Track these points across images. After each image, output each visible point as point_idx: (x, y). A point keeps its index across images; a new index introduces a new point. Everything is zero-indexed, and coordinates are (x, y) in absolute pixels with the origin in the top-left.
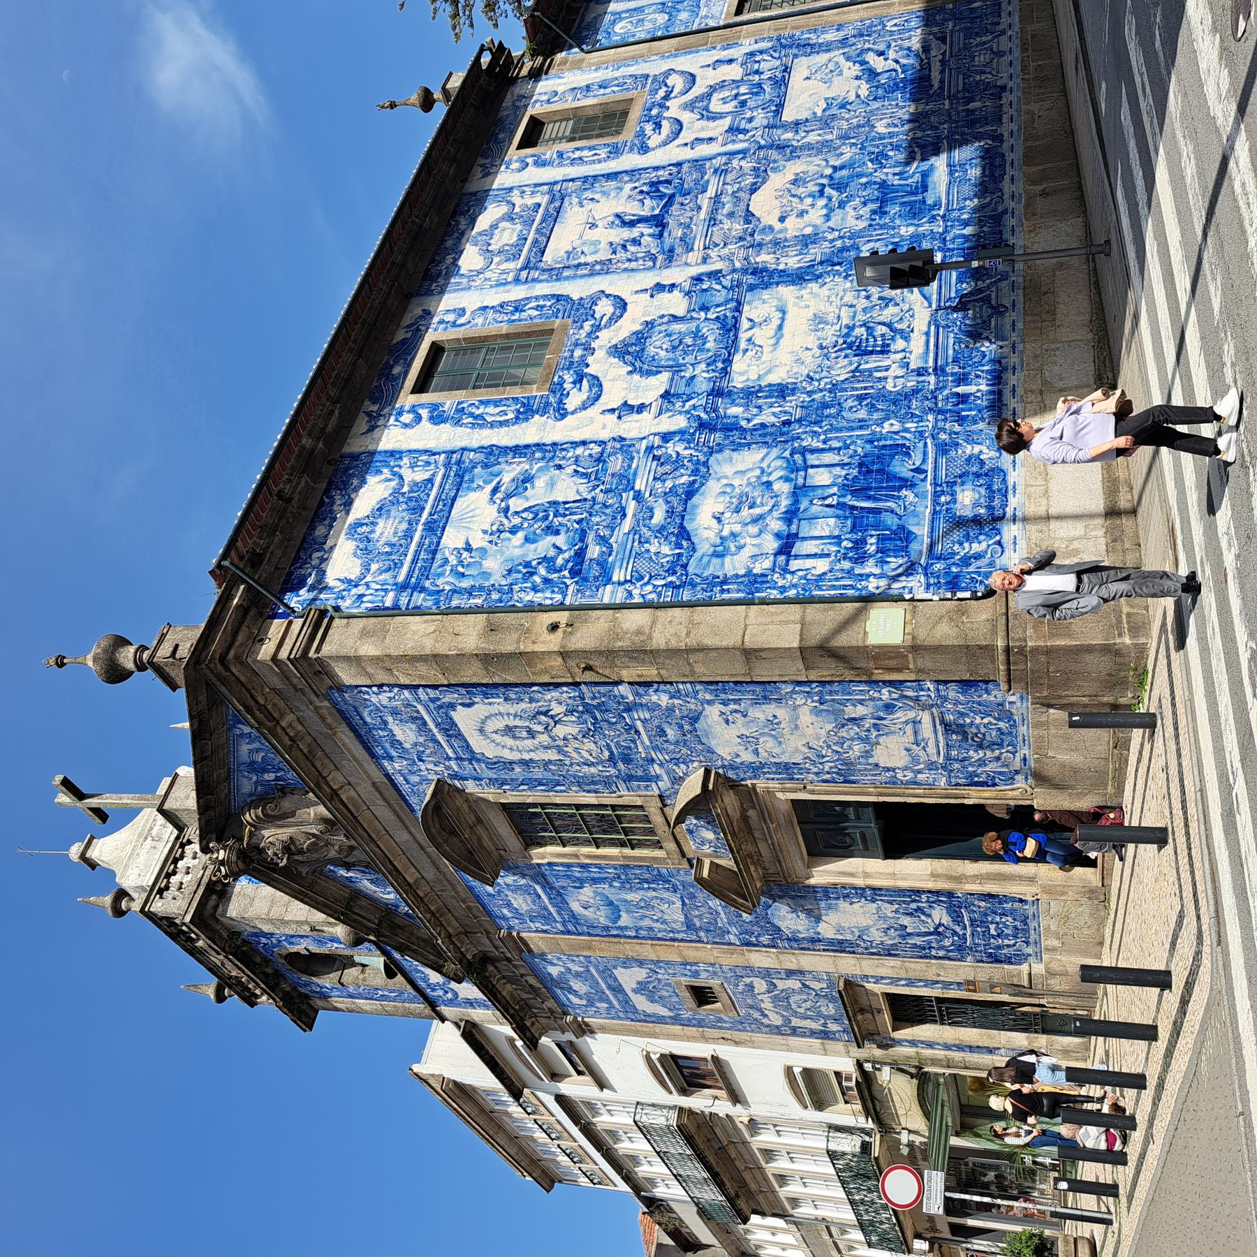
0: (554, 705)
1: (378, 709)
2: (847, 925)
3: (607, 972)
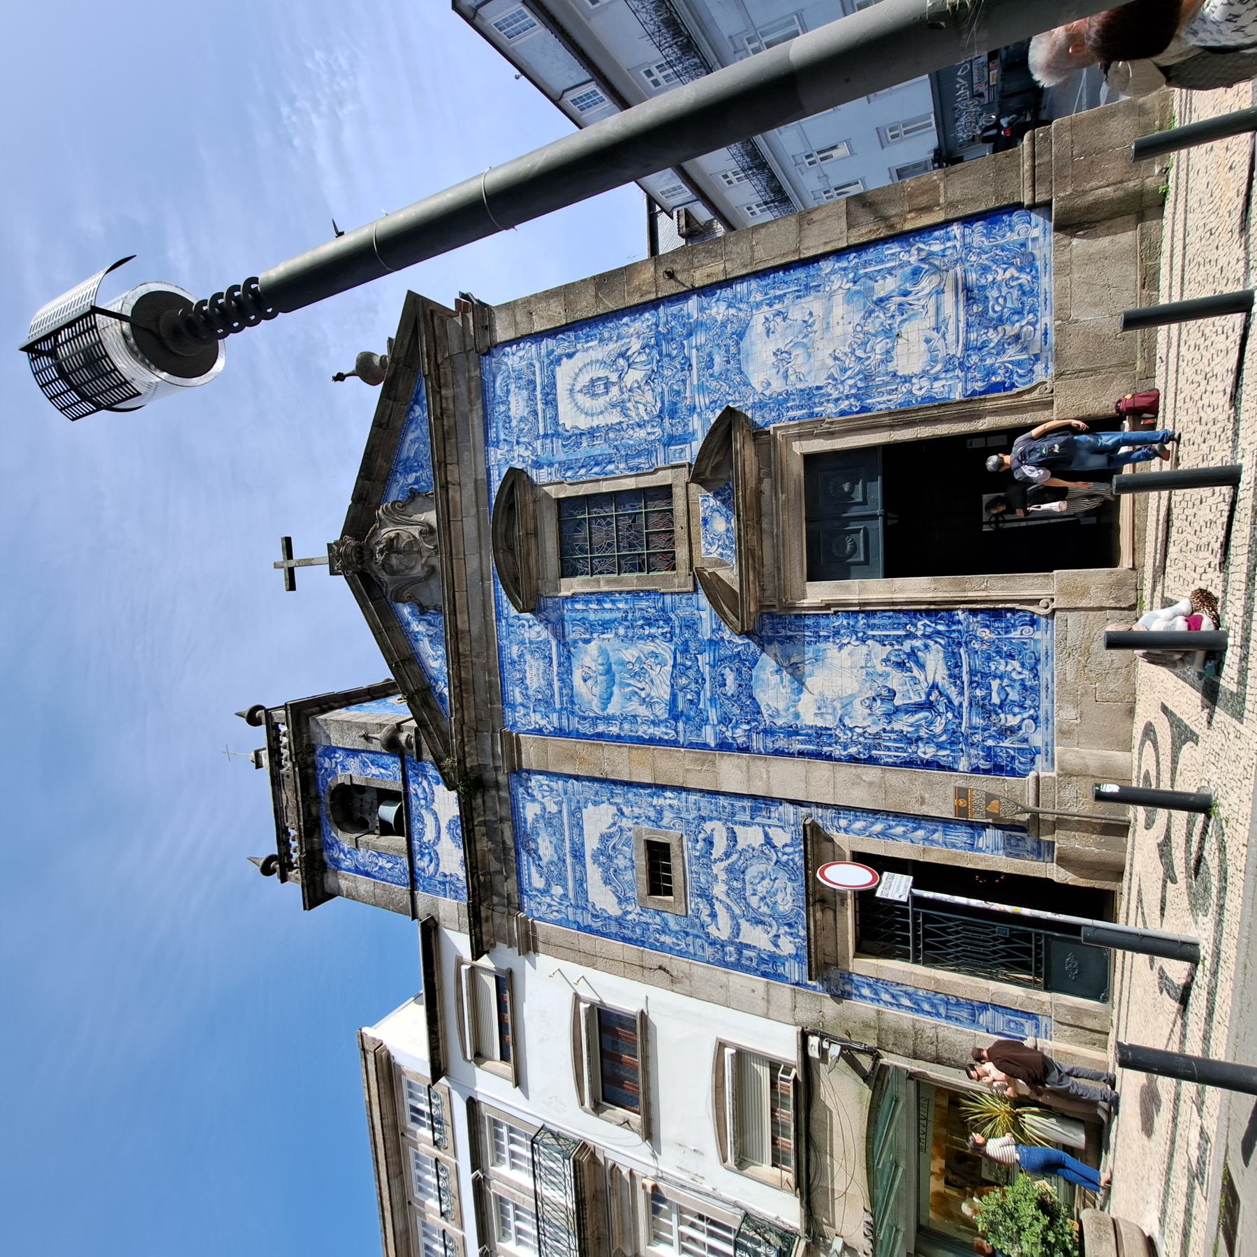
0: (634, 339)
1: (508, 377)
2: (829, 694)
3: (576, 813)
